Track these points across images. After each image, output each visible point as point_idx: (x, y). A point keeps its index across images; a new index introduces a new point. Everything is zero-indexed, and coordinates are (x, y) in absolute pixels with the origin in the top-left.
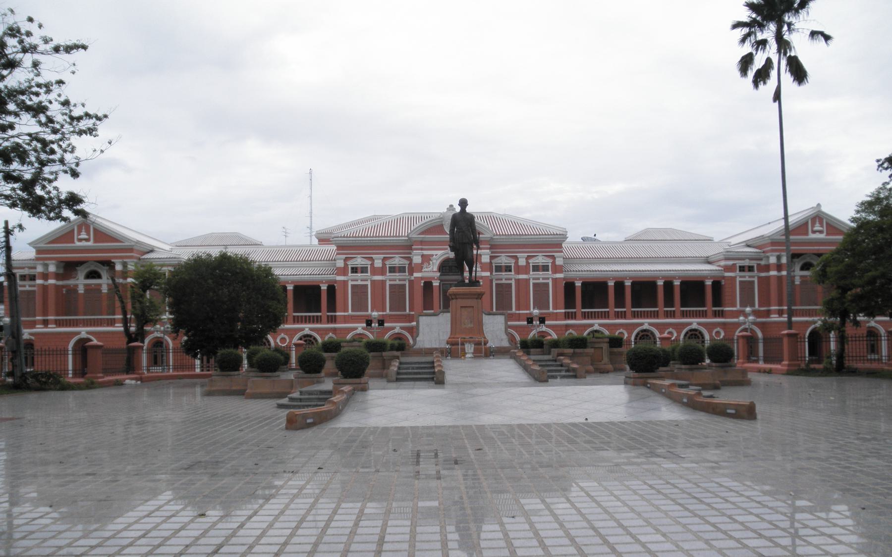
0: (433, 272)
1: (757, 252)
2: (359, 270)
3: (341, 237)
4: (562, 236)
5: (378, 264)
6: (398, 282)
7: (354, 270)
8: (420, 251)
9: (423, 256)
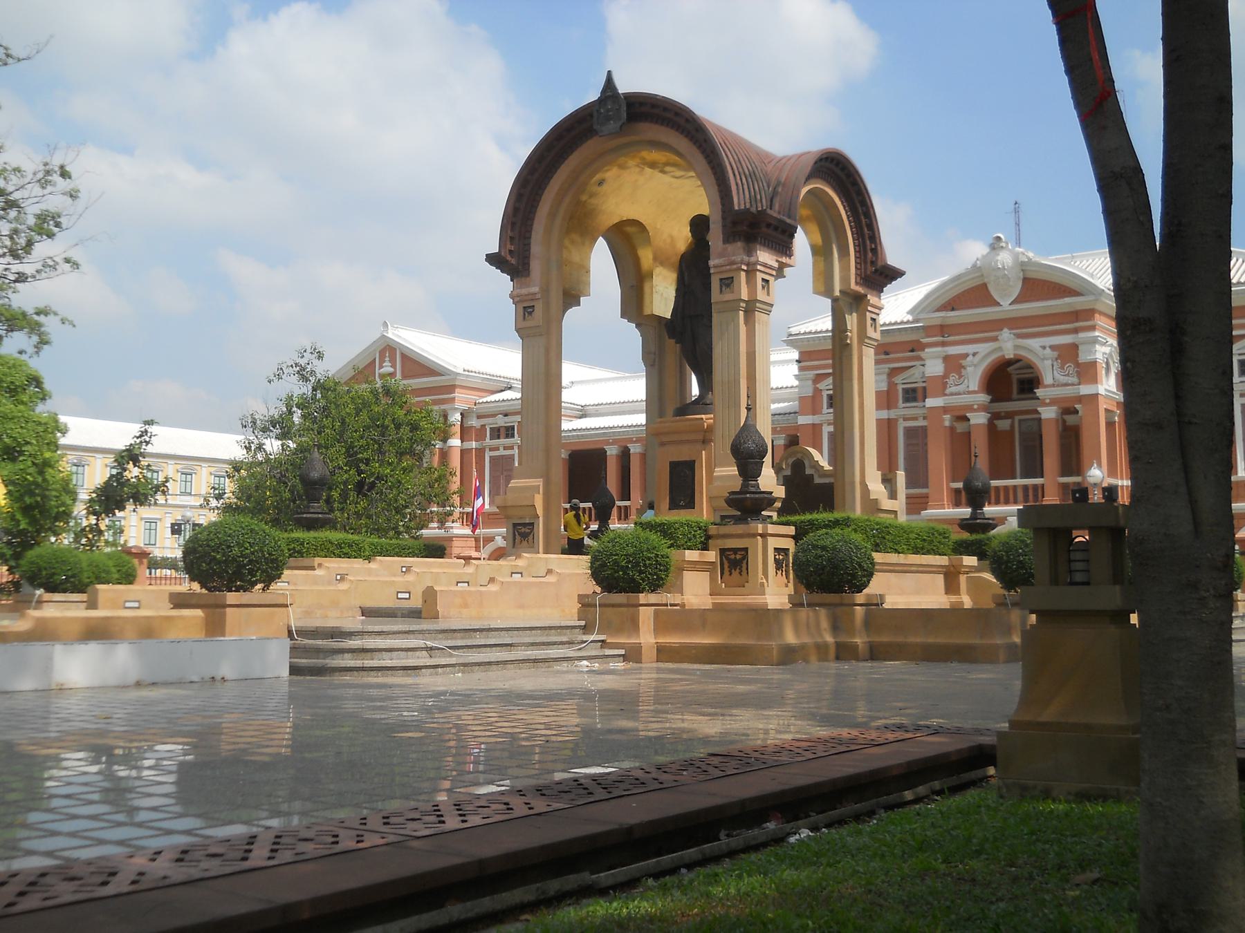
0: (970, 393)
8: (939, 349)
9: (947, 359)
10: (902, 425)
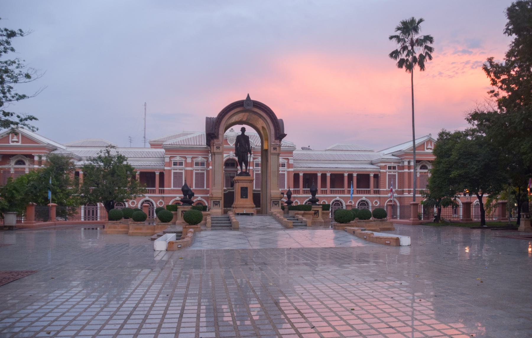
1: (398, 159)
2: (178, 164)
3: (168, 145)
4: (293, 148)
5: (189, 160)
6: (200, 171)
7: (175, 164)
10: (194, 172)
